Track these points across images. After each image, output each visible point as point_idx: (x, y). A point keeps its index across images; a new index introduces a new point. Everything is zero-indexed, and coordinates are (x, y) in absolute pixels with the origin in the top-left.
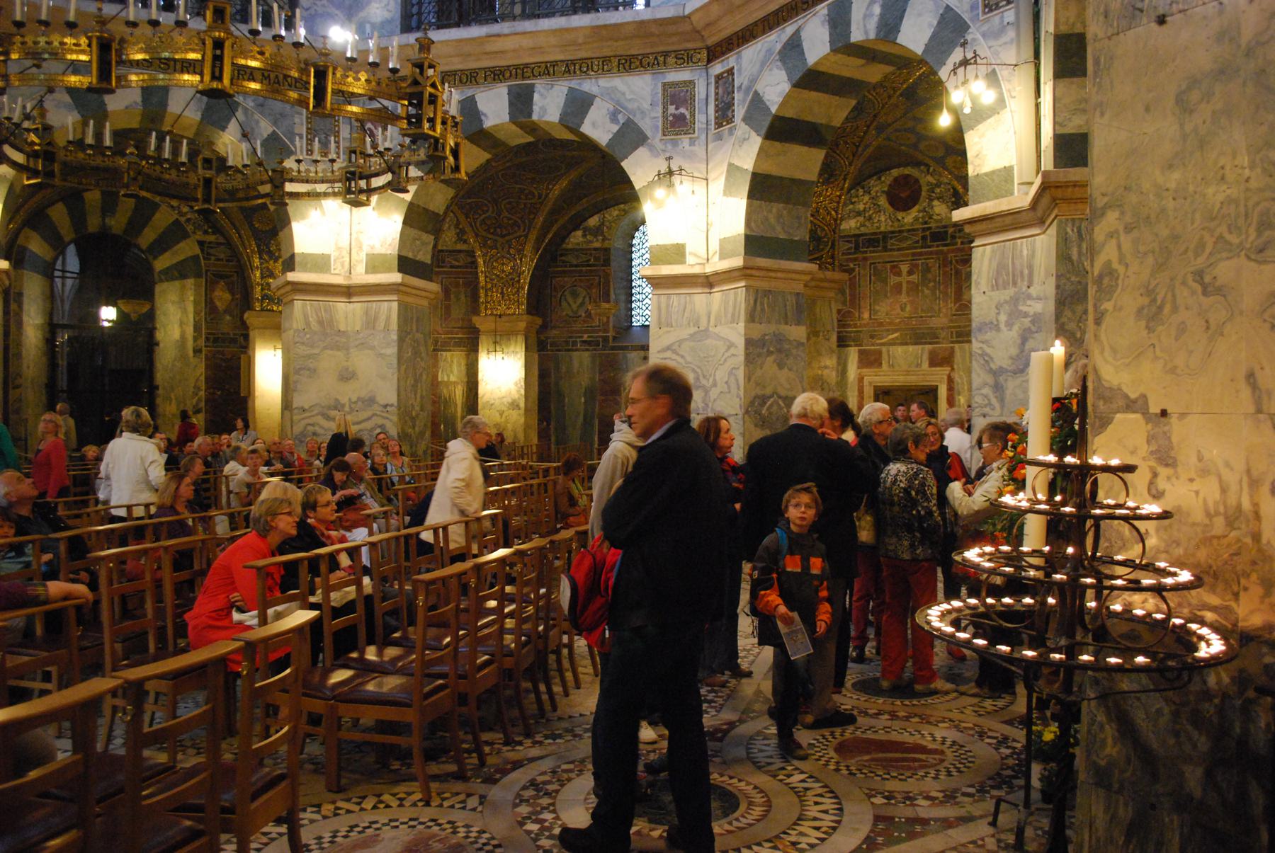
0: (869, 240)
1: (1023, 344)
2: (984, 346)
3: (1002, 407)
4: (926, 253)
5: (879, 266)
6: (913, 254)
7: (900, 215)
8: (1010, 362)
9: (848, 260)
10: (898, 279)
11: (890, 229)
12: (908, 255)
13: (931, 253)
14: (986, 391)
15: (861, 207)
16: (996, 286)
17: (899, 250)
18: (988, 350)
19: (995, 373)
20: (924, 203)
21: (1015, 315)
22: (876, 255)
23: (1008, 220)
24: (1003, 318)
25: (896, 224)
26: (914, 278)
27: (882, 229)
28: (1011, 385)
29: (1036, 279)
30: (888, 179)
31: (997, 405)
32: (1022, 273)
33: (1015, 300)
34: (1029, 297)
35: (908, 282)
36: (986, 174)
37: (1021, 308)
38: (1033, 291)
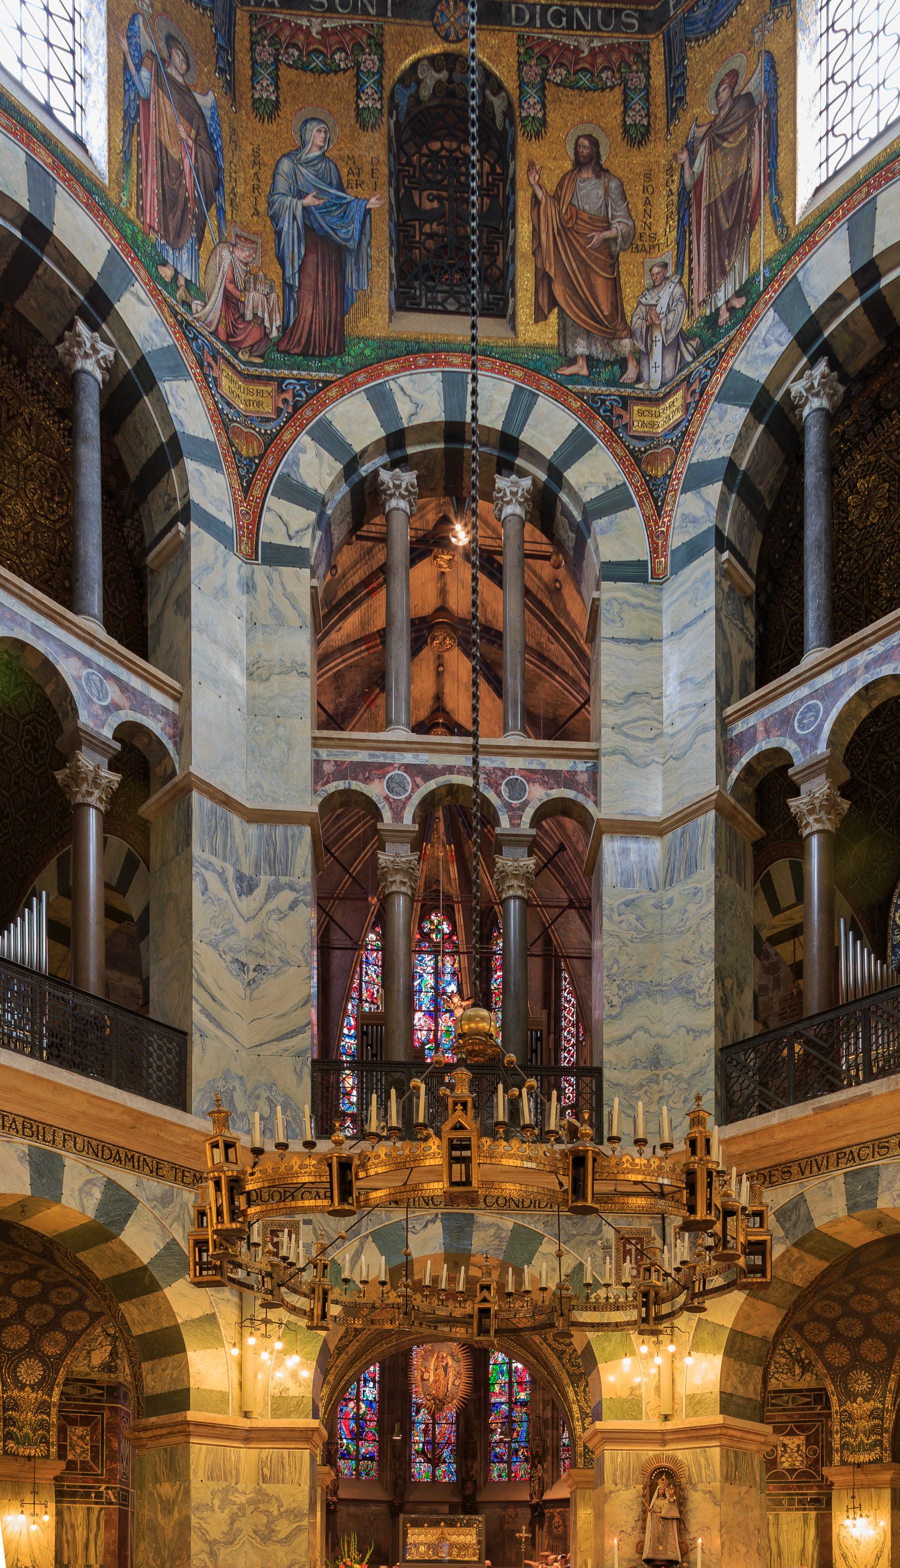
16: (211, 1478)
19: (211, 1543)
23: (226, 1432)
24: (217, 1502)
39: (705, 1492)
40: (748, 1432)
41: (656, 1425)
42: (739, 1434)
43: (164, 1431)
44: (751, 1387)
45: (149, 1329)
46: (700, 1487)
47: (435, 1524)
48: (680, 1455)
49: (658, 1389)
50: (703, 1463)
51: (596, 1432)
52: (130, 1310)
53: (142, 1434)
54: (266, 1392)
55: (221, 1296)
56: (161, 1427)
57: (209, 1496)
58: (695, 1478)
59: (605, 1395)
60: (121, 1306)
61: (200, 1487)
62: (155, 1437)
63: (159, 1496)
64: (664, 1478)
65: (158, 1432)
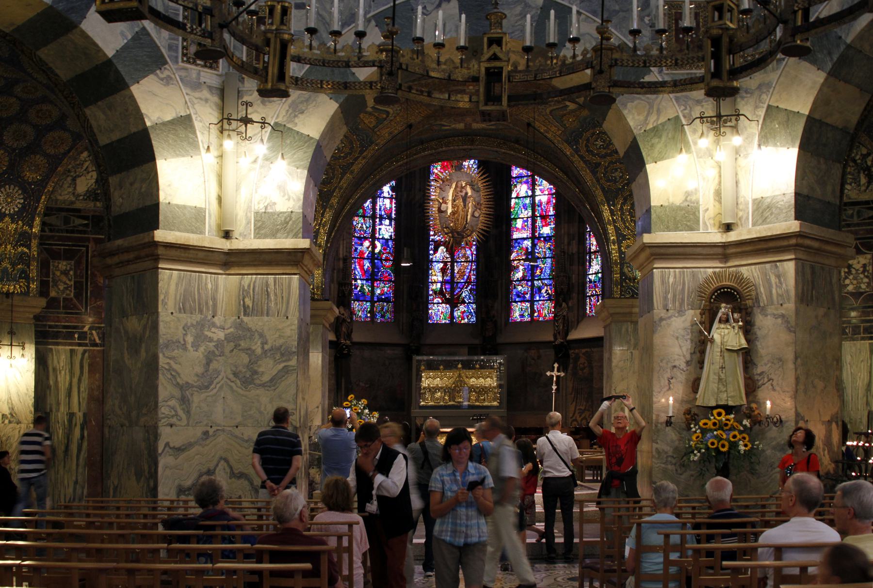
1: (208, 364)
2: (172, 362)
3: (188, 419)
8: (196, 379)
14: (173, 402)
16: (183, 310)
18: (175, 366)
19: (181, 387)
21: (200, 339)
23: (201, 255)
24: (190, 339)
28: (197, 399)
29: (219, 313)
31: (184, 416)
32: (207, 303)
33: (201, 325)
34: (214, 325)
36: (178, 206)
37: (206, 333)
38: (216, 320)
39: (776, 316)
40: (827, 242)
41: (717, 237)
42: (816, 244)
43: (132, 256)
44: (829, 188)
45: (116, 136)
46: (770, 310)
47: (449, 366)
48: (744, 270)
49: (718, 194)
50: (777, 281)
51: (645, 247)
52: (97, 116)
53: (109, 261)
54: (249, 207)
55: (197, 94)
56: (127, 250)
57: (181, 332)
58: (764, 298)
59: (655, 201)
60: (88, 111)
61: (170, 319)
62: (122, 264)
63: (126, 332)
64: (728, 300)
65: (125, 257)
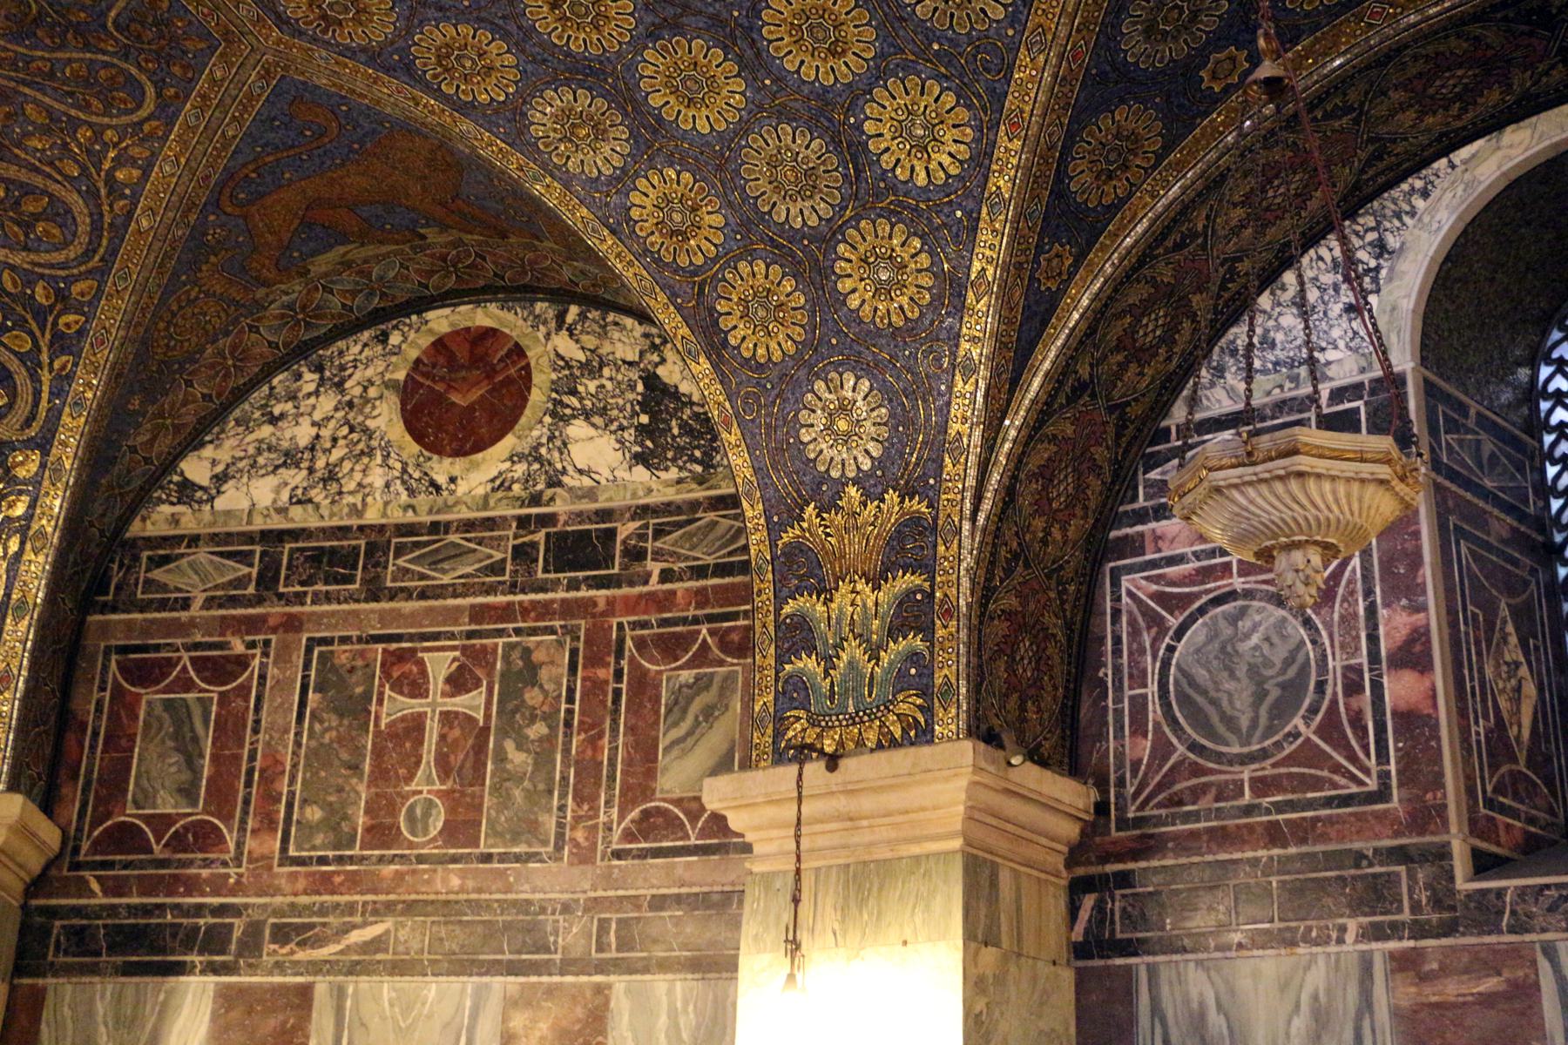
0: (316, 557)
4: (525, 611)
5: (343, 655)
6: (478, 614)
7: (441, 469)
9: (225, 624)
10: (414, 705)
11: (397, 516)
12: (453, 615)
13: (545, 610)
15: (303, 433)
17: (423, 595)
20: (532, 428)
22: (336, 613)
25: (423, 500)
26: (472, 703)
27: (372, 516)
30: (413, 340)
35: (448, 718)
